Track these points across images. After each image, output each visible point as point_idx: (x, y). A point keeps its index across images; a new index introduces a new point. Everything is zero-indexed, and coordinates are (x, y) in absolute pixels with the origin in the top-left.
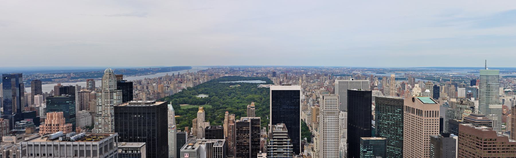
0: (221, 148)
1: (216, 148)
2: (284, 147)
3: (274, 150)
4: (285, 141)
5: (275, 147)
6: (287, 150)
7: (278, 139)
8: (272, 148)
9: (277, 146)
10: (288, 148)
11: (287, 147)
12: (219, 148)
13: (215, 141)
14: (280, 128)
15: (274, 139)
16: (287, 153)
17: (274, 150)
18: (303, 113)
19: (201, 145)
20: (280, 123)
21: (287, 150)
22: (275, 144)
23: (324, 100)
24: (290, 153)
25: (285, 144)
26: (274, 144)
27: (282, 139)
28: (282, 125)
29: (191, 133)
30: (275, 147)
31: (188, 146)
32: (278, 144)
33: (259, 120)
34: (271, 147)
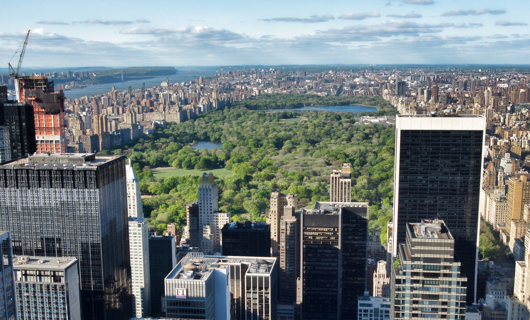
0: (267, 279)
1: (255, 278)
2: (443, 282)
3: (412, 289)
4: (445, 267)
5: (417, 282)
6: (450, 290)
7: (426, 260)
9: (421, 278)
10: (454, 286)
11: (450, 283)
12: (261, 278)
13: (250, 260)
15: (413, 259)
20: (432, 217)
22: (417, 274)
25: (445, 275)
26: (413, 274)
27: (438, 260)
28: (436, 224)
30: (417, 282)
32: (425, 275)
33: (364, 210)
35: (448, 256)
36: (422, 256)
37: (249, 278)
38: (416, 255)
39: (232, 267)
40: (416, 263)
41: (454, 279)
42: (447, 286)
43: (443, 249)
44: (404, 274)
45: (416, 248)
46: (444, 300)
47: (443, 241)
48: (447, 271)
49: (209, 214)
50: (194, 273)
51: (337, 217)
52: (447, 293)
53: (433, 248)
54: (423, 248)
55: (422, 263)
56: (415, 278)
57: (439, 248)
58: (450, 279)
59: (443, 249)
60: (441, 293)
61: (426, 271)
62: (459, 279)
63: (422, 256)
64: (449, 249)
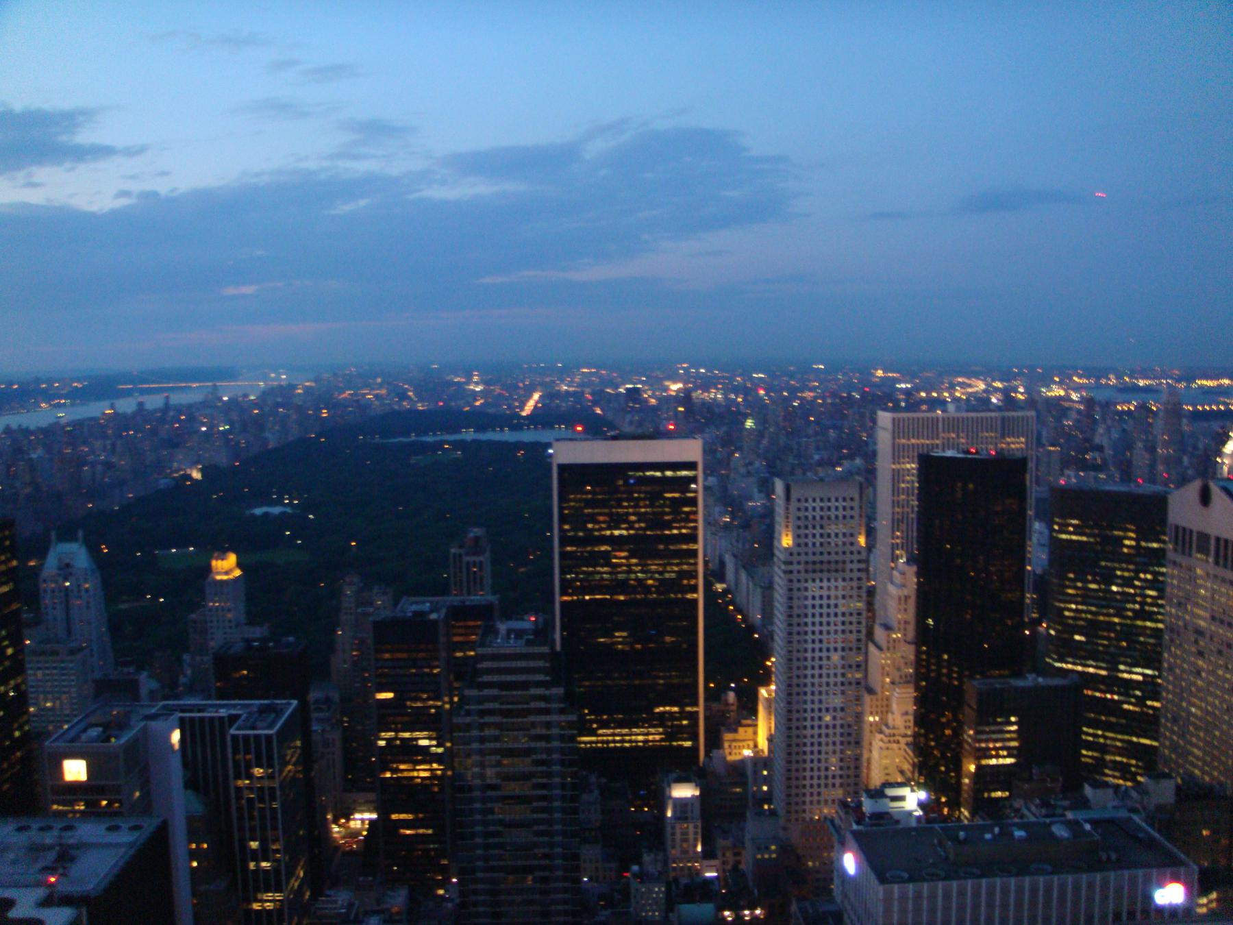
0: (269, 737)
1: (246, 737)
2: (534, 725)
3: (482, 740)
6: (547, 738)
7: (502, 686)
8: (475, 733)
11: (548, 725)
12: (257, 737)
14: (519, 634)
16: (549, 751)
17: (482, 740)
18: (743, 576)
19: (153, 724)
21: (547, 738)
22: (491, 712)
23: (794, 505)
24: (562, 751)
26: (483, 713)
27: (525, 685)
29: (182, 680)
31: (85, 730)
32: (503, 713)
34: (468, 727)
35: (541, 677)
36: (496, 678)
37: (234, 737)
38: (486, 678)
39: (212, 719)
40: (486, 692)
41: (554, 718)
42: (544, 732)
43: (532, 664)
44: (468, 713)
45: (485, 665)
46: (539, 757)
47: (531, 650)
48: (543, 705)
49: (228, 630)
50: (104, 732)
51: (435, 622)
52: (543, 744)
53: (514, 664)
54: (495, 665)
55: (495, 692)
56: (487, 719)
57: (522, 664)
58: (548, 718)
59: (532, 664)
60: (533, 745)
61: (504, 707)
62: (563, 717)
63: (496, 678)
64: (541, 664)
